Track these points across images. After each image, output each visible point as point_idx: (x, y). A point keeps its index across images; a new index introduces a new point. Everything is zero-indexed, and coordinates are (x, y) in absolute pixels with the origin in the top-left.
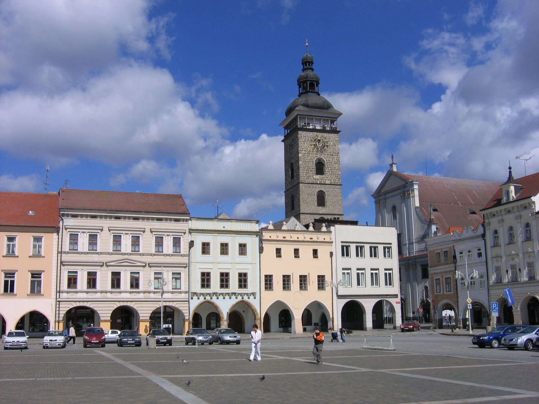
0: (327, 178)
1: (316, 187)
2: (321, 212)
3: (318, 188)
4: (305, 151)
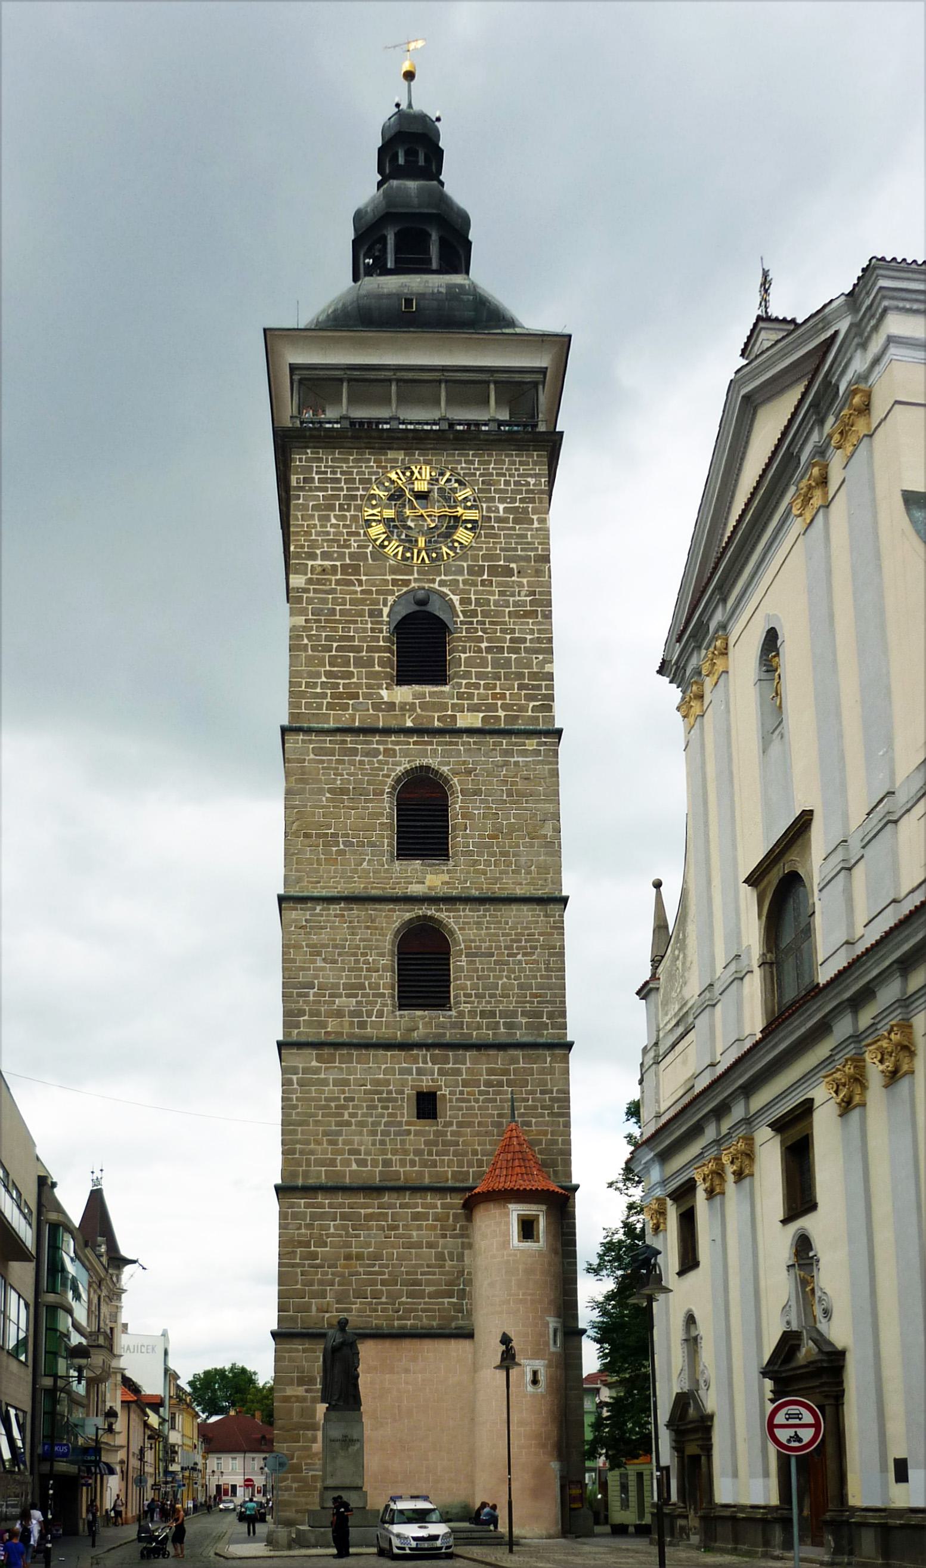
0: (462, 699)
2: (416, 889)
3: (404, 757)
4: (326, 556)
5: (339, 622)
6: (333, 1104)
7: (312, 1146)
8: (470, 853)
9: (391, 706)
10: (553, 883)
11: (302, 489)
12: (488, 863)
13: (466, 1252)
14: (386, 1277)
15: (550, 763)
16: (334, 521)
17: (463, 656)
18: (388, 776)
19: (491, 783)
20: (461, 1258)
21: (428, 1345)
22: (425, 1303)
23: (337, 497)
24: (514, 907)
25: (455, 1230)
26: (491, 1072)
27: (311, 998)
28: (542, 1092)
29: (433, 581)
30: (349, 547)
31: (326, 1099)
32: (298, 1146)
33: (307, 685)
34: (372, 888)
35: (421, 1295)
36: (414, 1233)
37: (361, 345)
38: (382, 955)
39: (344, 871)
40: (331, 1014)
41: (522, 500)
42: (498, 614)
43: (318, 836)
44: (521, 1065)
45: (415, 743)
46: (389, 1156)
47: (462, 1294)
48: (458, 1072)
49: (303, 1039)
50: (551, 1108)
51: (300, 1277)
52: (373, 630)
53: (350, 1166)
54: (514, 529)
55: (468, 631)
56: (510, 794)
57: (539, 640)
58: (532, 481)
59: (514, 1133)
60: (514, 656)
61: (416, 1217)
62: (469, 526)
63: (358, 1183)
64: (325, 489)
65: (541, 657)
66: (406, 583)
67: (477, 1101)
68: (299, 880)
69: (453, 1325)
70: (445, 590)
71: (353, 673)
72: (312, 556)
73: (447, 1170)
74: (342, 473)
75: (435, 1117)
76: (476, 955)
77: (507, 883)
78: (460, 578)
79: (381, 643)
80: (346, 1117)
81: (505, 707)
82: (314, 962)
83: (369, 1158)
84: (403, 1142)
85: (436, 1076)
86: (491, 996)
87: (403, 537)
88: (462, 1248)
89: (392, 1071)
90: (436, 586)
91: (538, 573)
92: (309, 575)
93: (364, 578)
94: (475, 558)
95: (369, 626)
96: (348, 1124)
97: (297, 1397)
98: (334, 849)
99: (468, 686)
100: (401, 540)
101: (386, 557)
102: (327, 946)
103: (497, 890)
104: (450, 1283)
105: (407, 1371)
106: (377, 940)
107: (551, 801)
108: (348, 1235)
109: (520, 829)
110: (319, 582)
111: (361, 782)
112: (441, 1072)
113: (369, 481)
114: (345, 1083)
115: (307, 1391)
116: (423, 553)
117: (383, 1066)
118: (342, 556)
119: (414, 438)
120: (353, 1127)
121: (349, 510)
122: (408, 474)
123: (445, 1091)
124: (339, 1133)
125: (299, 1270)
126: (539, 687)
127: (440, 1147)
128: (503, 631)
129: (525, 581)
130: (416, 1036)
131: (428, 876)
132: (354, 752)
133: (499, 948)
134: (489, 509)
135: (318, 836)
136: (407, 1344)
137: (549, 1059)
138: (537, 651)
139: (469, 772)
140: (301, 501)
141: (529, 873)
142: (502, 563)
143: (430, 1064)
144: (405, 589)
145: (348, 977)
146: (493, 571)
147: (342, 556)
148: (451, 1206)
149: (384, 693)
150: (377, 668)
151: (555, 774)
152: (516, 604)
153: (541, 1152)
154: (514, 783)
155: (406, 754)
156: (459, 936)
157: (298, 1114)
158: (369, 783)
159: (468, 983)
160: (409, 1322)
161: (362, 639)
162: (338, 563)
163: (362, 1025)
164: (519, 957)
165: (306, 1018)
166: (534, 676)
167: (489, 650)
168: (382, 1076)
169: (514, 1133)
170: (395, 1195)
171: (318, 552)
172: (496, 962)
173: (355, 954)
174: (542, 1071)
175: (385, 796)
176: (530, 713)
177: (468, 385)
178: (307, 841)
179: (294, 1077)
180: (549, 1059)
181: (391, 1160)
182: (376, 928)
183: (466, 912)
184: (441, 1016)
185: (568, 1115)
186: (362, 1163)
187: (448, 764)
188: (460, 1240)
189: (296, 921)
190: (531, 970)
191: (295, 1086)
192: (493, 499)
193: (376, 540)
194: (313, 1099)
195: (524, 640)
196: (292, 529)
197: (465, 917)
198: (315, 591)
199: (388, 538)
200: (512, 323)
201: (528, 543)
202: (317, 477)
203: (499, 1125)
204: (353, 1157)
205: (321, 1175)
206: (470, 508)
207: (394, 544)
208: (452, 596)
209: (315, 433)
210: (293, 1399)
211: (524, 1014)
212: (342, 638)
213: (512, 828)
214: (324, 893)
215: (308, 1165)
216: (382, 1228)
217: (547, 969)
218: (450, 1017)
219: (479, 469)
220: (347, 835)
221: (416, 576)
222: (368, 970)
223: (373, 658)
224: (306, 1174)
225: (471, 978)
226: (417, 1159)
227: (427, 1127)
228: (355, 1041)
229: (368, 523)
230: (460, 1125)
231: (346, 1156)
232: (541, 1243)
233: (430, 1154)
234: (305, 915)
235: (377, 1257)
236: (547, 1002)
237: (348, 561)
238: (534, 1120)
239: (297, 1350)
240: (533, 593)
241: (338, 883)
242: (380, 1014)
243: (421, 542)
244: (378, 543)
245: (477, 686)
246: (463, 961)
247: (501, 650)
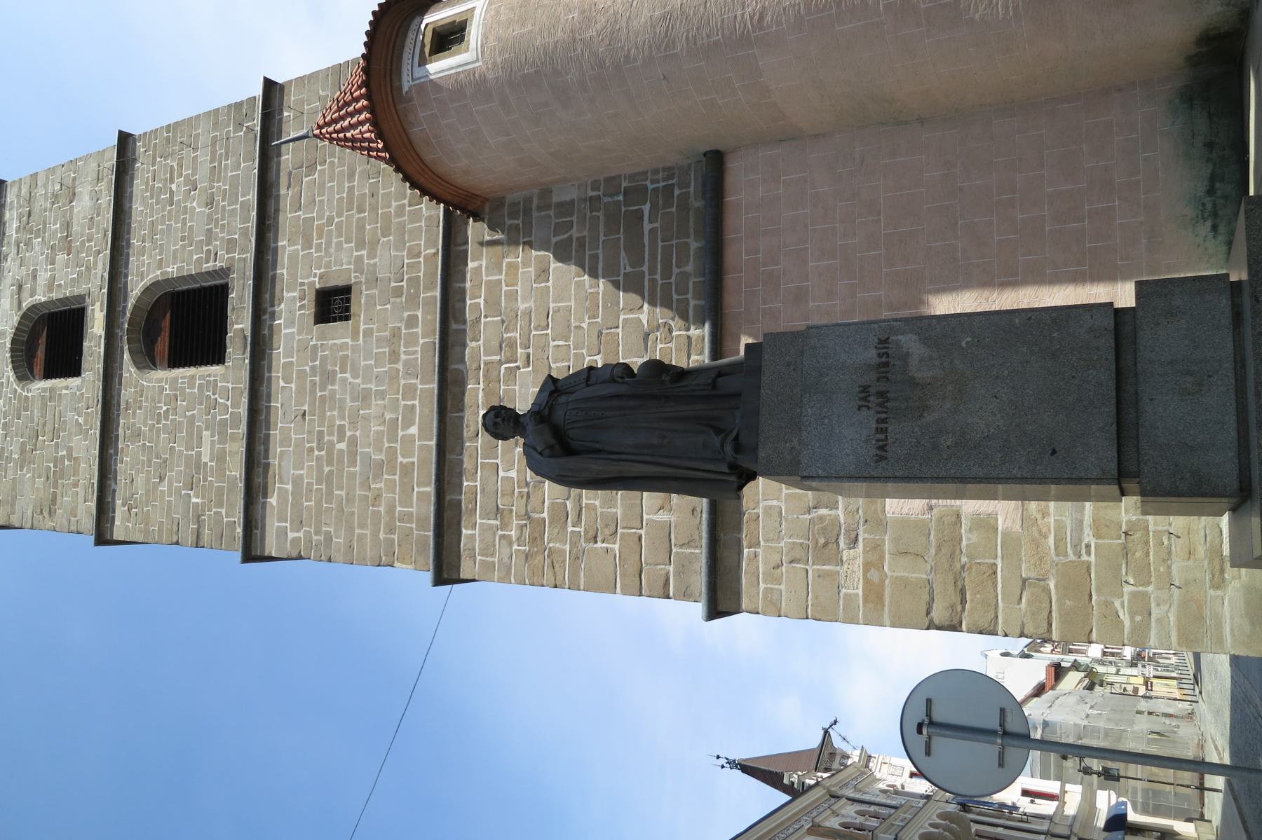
20: (566, 208)
22: (652, 271)
32: (382, 536)
36: (522, 306)
47: (636, 193)
53: (411, 439)
69: (697, 204)
88: (548, 207)
96: (353, 442)
97: (867, 567)
117: (282, 383)
120: (358, 433)
160: (692, 303)
164: (174, 187)
165: (223, 511)
168: (293, 386)
179: (291, 535)
188: (535, 214)
191: (301, 534)
194: (319, 503)
210: (874, 575)
227: (359, 303)
230: (360, 246)
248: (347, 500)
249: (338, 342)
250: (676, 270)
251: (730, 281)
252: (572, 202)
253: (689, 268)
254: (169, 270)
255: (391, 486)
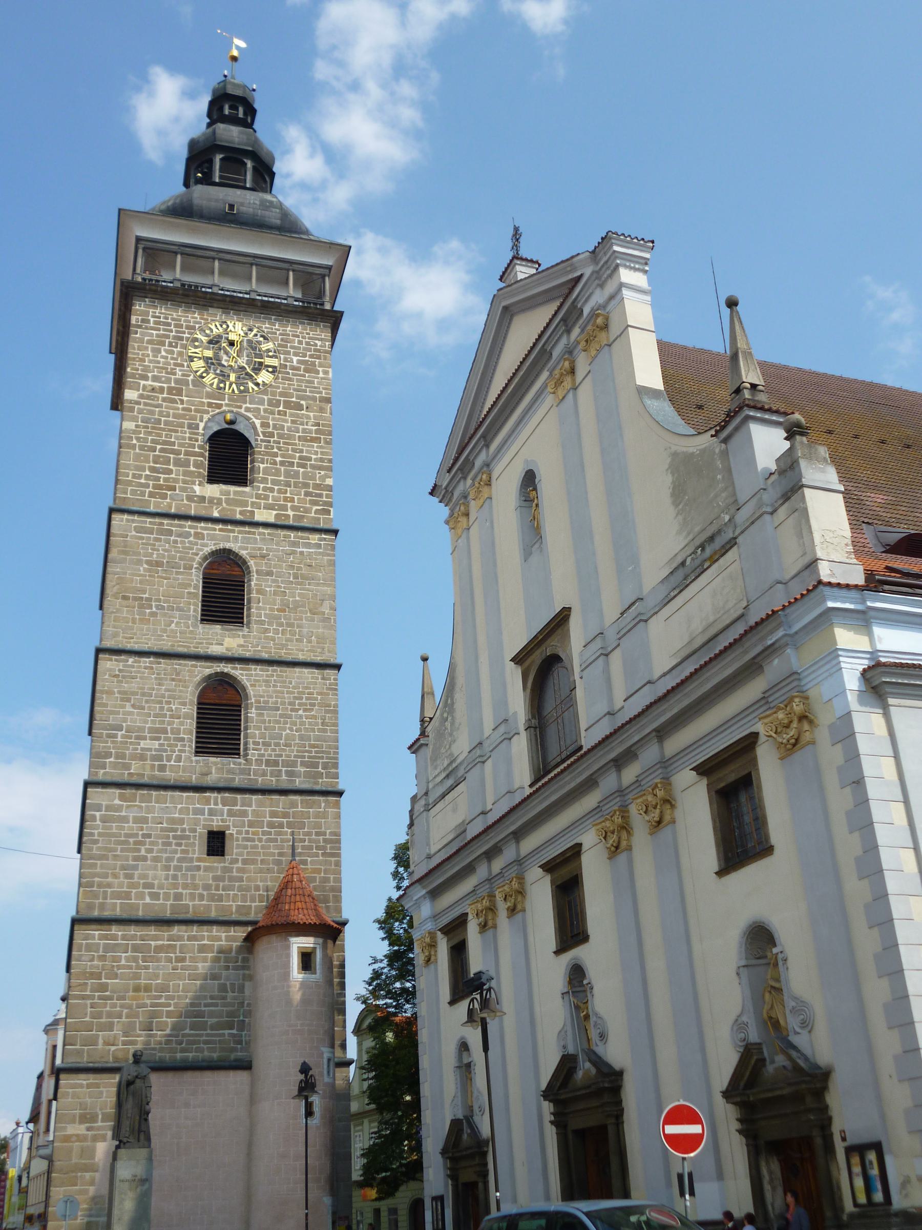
1: (198, 536)
2: (215, 650)
4: (155, 379)
5: (164, 430)
6: (131, 840)
7: (110, 879)
8: (262, 623)
9: (202, 499)
10: (329, 652)
11: (140, 327)
12: (276, 632)
13: (247, 984)
14: (172, 1008)
15: (329, 555)
16: (163, 353)
17: (262, 466)
18: (197, 554)
19: (281, 567)
20: (242, 989)
21: (208, 1076)
22: (207, 1035)
23: (168, 337)
24: (297, 670)
25: (237, 962)
26: (273, 814)
27: (119, 739)
28: (317, 834)
29: (240, 407)
30: (175, 374)
31: (127, 835)
32: (97, 879)
33: (134, 476)
34: (179, 646)
35: (203, 1026)
36: (200, 965)
37: (193, 231)
38: (184, 704)
39: (155, 630)
40: (134, 757)
41: (311, 356)
42: (290, 437)
43: (135, 599)
44: (300, 809)
45: (220, 530)
46: (180, 890)
47: (242, 1026)
48: (244, 814)
49: (108, 779)
50: (324, 848)
51: (89, 1010)
52: (190, 439)
53: (144, 899)
54: (304, 376)
55: (266, 447)
56: (296, 577)
57: (322, 460)
58: (319, 343)
59: (295, 871)
60: (302, 470)
61: (202, 949)
62: (270, 369)
63: (150, 915)
64: (159, 330)
65: (323, 473)
66: (219, 406)
67: (260, 840)
68: (116, 635)
69: (232, 1057)
70: (249, 415)
71: (172, 470)
72: (145, 378)
73: (232, 906)
74: (173, 319)
75: (222, 854)
76: (264, 708)
77: (292, 650)
78: (262, 407)
79: (197, 450)
80: (143, 853)
81: (294, 508)
82: (124, 707)
83: (162, 892)
84: (193, 877)
85: (225, 817)
86: (277, 745)
87: (218, 372)
88: (243, 980)
89: (185, 811)
90: (242, 411)
91: (322, 410)
92: (141, 392)
93: (185, 399)
94: (274, 394)
95: (188, 435)
96: (145, 859)
97: (77, 1135)
98: (148, 611)
99: (265, 489)
100: (216, 374)
101: (204, 385)
102: (136, 694)
103: (284, 655)
104: (231, 1014)
105: (187, 1105)
106: (180, 691)
107: (329, 585)
108: (138, 967)
109: (304, 606)
110: (148, 397)
111: (174, 557)
112: (231, 813)
113: (193, 328)
114: (145, 820)
115: (88, 1129)
116: (234, 386)
118: (168, 381)
119: (230, 302)
120: (149, 862)
121: (176, 347)
122: (224, 326)
123: (231, 831)
124: (135, 868)
125: (89, 1002)
126: (320, 496)
127: (226, 883)
128: (293, 450)
129: (311, 414)
130: (210, 780)
131: (227, 639)
132: (170, 533)
133: (283, 703)
134: (286, 360)
135: (135, 599)
136: (189, 1076)
137: (323, 805)
138: (320, 468)
139: (263, 557)
140: (138, 336)
141: (310, 642)
142: (294, 399)
143: (220, 806)
144: (218, 411)
145: (153, 722)
146: (288, 405)
147: (168, 381)
148: (233, 939)
149: (197, 488)
150: (192, 468)
151: (332, 563)
152: (304, 431)
153: (315, 888)
154: (299, 569)
155: (212, 537)
156: (251, 691)
157: (98, 848)
158: (180, 559)
159: (257, 732)
160: (191, 1055)
161: (180, 445)
162: (165, 385)
163: (162, 768)
164: (301, 712)
165: (112, 760)
166: (317, 486)
167: (282, 463)
168: (177, 815)
169: (295, 871)
170: (184, 928)
171: (150, 375)
172: (281, 716)
173: (160, 702)
174: (317, 815)
175: (194, 570)
176: (313, 515)
177: (275, 269)
178: (125, 603)
180: (323, 805)
181: (182, 894)
182: (180, 681)
183: (257, 671)
184: (231, 763)
185: (338, 855)
186: (155, 896)
187: (246, 549)
188: (241, 972)
189: (110, 670)
190: (310, 724)
191: (98, 822)
192: (289, 353)
193: (197, 372)
194: (114, 835)
195: (310, 459)
196: (130, 355)
197: (256, 675)
198: (145, 404)
199: (207, 372)
200: (307, 232)
201: (315, 388)
202: (152, 320)
203: (278, 863)
204: (146, 891)
205: (116, 908)
206: (271, 357)
207: (211, 376)
208: (254, 420)
209: (153, 288)
210: (74, 1139)
211: (303, 764)
212: (165, 443)
213: (297, 605)
214: (136, 647)
215: (105, 898)
216: (169, 960)
217: (323, 724)
218: (240, 764)
219: (278, 330)
220: (159, 600)
221: (227, 402)
222: (172, 716)
223: (189, 461)
224: (102, 906)
225: (259, 728)
226: (205, 893)
227: (215, 862)
228: (155, 782)
229: (191, 359)
230: (245, 862)
231: (141, 890)
232: (318, 976)
233: (217, 889)
234: (118, 666)
235: (164, 988)
236: (323, 752)
237: (173, 385)
238: (309, 859)
239: (81, 1086)
240: (318, 424)
241: (149, 639)
242: (179, 759)
243: (233, 377)
244: (198, 374)
245: (272, 490)
246: (253, 713)
247: (292, 464)
248: (115, 856)
249: (197, 848)
250: (205, 1046)
251: (197, 1074)
252: (243, 992)
253: (206, 1053)
254: (253, 710)
255: (121, 885)
